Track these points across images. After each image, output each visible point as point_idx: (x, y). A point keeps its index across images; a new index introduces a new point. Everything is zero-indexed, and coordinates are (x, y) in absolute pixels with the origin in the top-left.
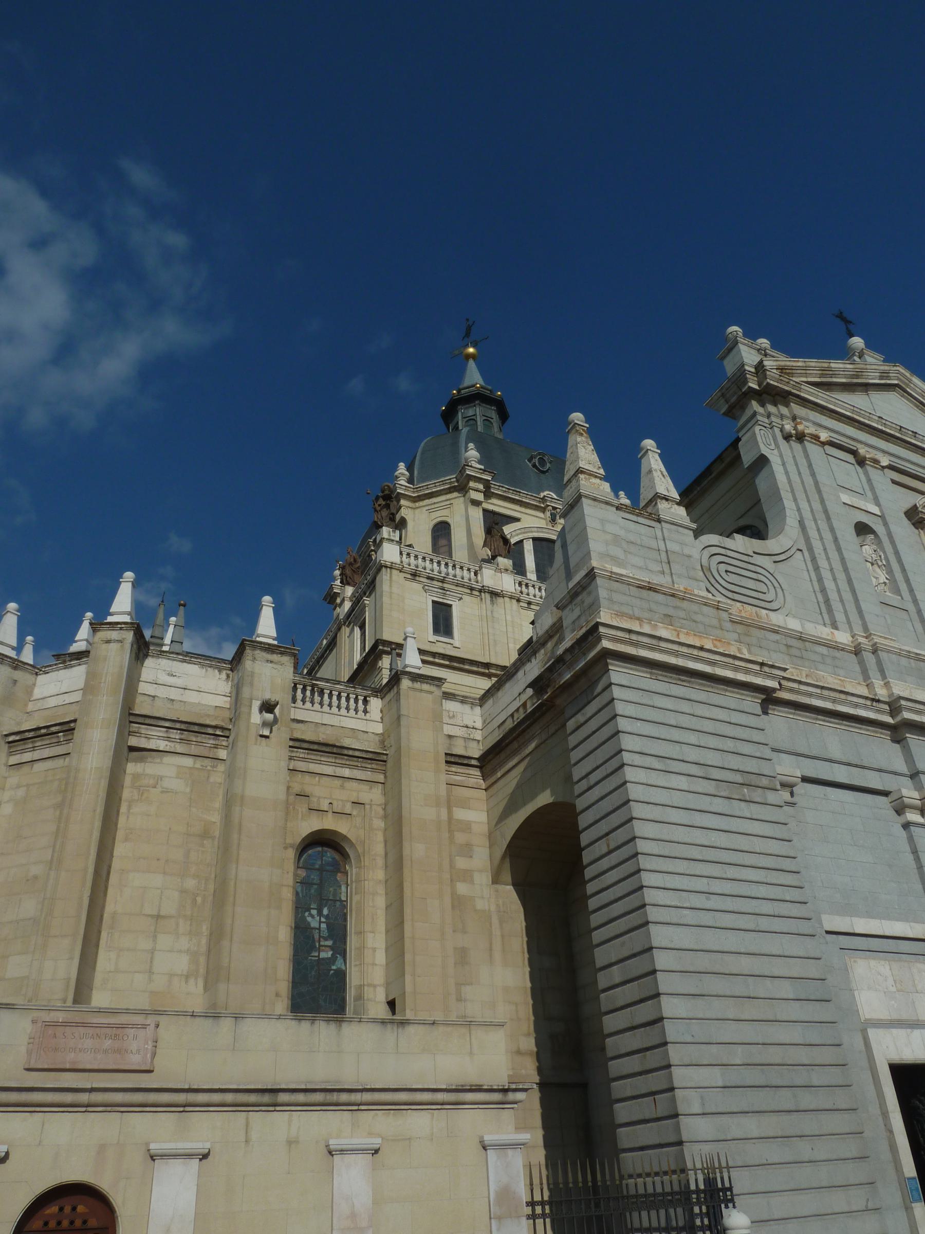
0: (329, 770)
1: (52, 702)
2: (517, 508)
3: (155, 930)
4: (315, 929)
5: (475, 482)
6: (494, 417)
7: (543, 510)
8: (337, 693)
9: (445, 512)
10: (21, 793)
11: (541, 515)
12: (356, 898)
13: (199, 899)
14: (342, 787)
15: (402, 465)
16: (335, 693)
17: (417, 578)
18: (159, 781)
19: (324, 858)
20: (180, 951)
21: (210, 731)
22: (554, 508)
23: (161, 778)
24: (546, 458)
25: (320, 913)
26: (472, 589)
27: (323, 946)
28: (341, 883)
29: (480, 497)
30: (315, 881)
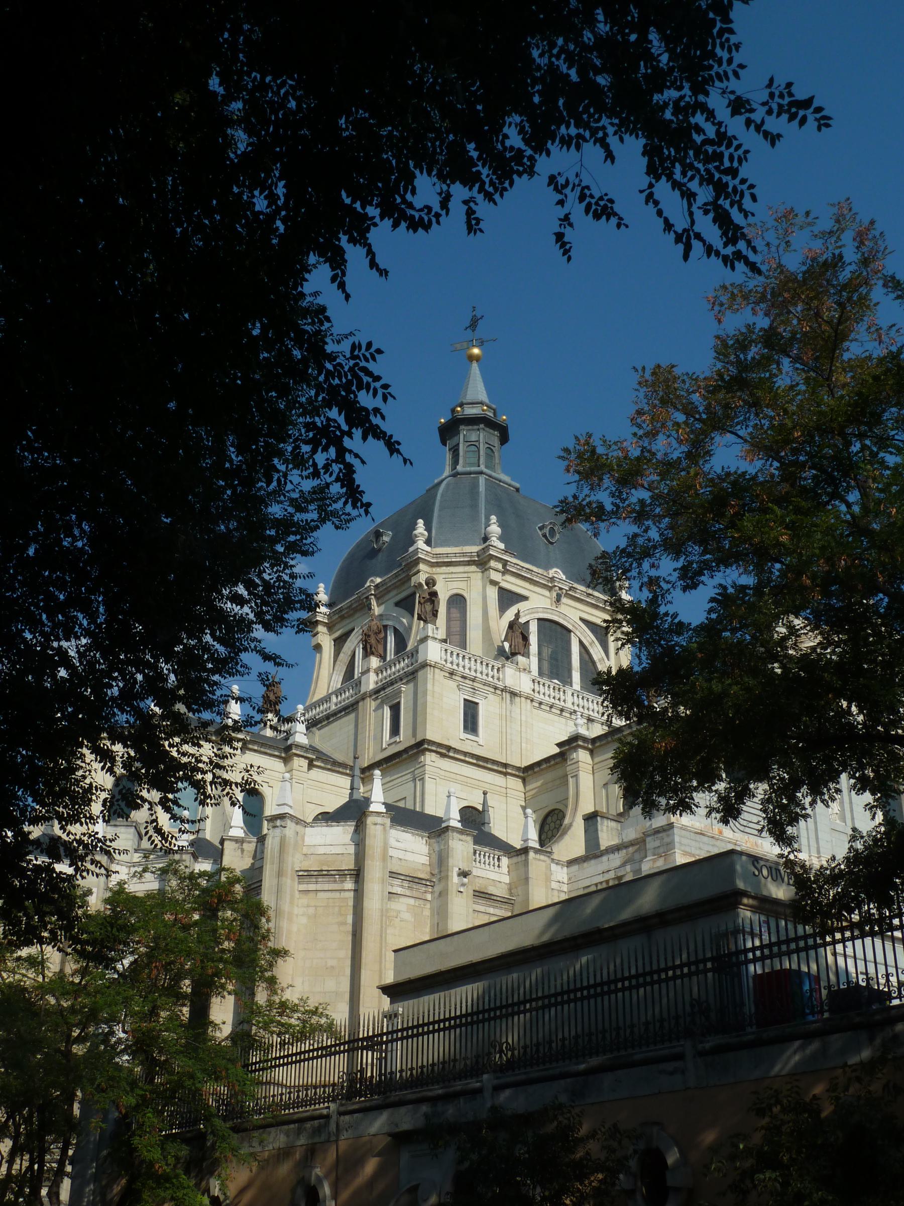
1: (322, 850)
2: (526, 585)
5: (496, 561)
6: (496, 445)
7: (550, 589)
9: (462, 585)
10: (311, 911)
11: (547, 593)
15: (421, 522)
17: (454, 677)
21: (424, 882)
22: (561, 589)
23: (399, 912)
24: (556, 528)
26: (496, 688)
29: (495, 576)
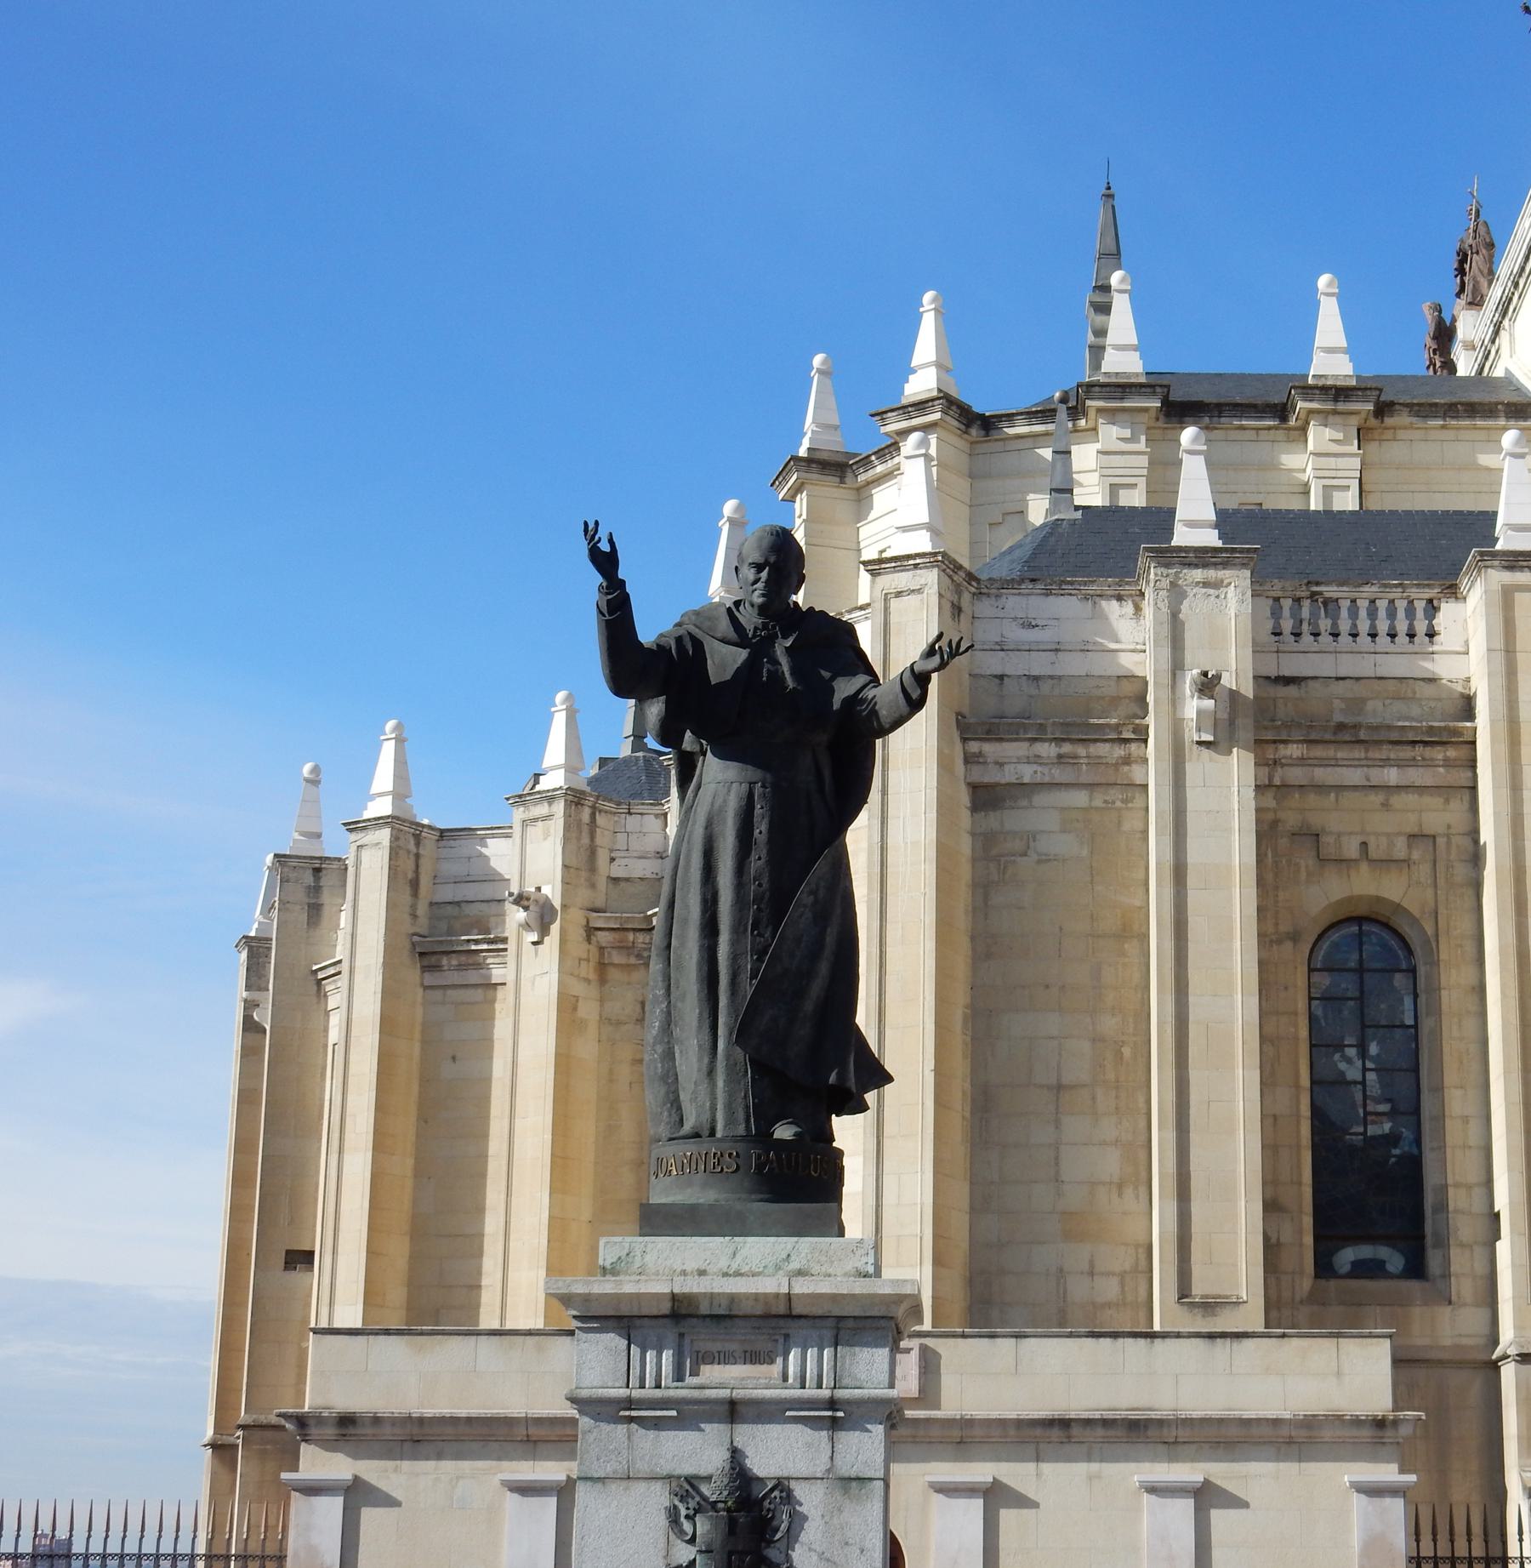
0: (1354, 776)
3: (1057, 1108)
4: (1355, 1083)
8: (1366, 603)
12: (1426, 1025)
13: (1127, 1051)
14: (1386, 805)
16: (1363, 605)
18: (1032, 844)
19: (1364, 947)
20: (1103, 1143)
23: (1033, 836)
25: (1363, 1053)
27: (1372, 1113)
28: (1403, 992)
30: (1349, 994)
